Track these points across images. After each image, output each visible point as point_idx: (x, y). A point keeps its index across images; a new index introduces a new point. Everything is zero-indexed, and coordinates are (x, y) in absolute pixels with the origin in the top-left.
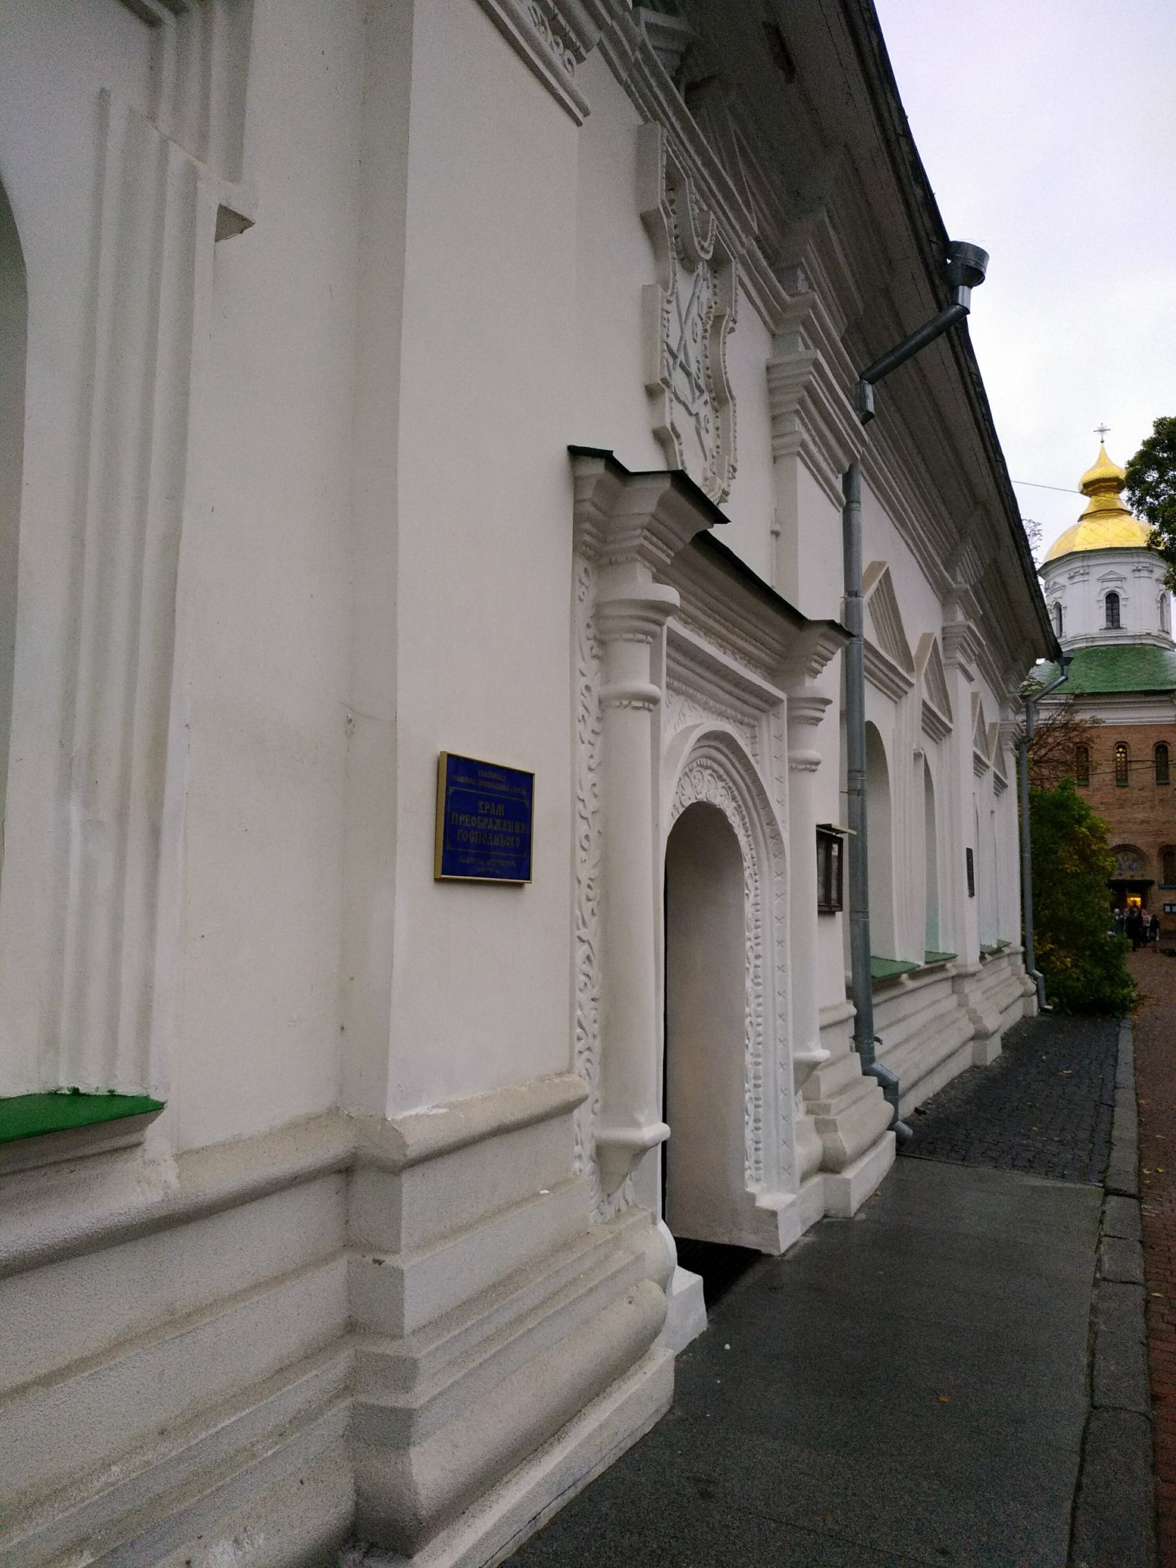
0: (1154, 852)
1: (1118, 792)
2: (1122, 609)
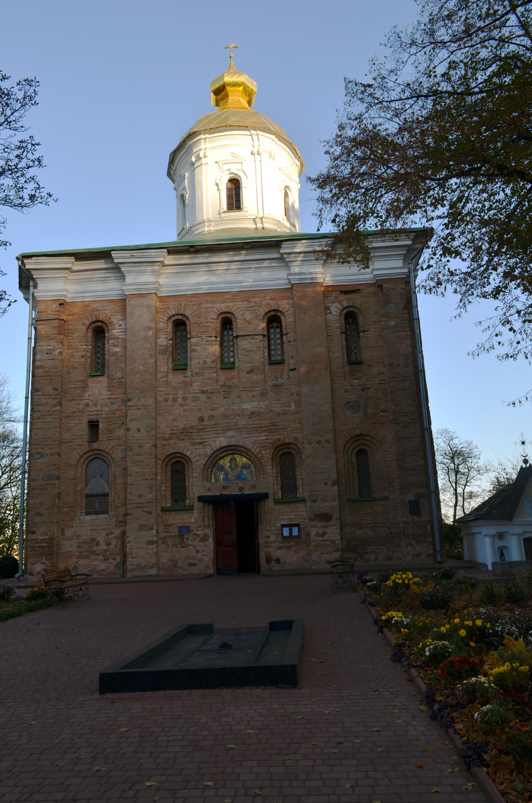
0: (267, 454)
1: (223, 376)
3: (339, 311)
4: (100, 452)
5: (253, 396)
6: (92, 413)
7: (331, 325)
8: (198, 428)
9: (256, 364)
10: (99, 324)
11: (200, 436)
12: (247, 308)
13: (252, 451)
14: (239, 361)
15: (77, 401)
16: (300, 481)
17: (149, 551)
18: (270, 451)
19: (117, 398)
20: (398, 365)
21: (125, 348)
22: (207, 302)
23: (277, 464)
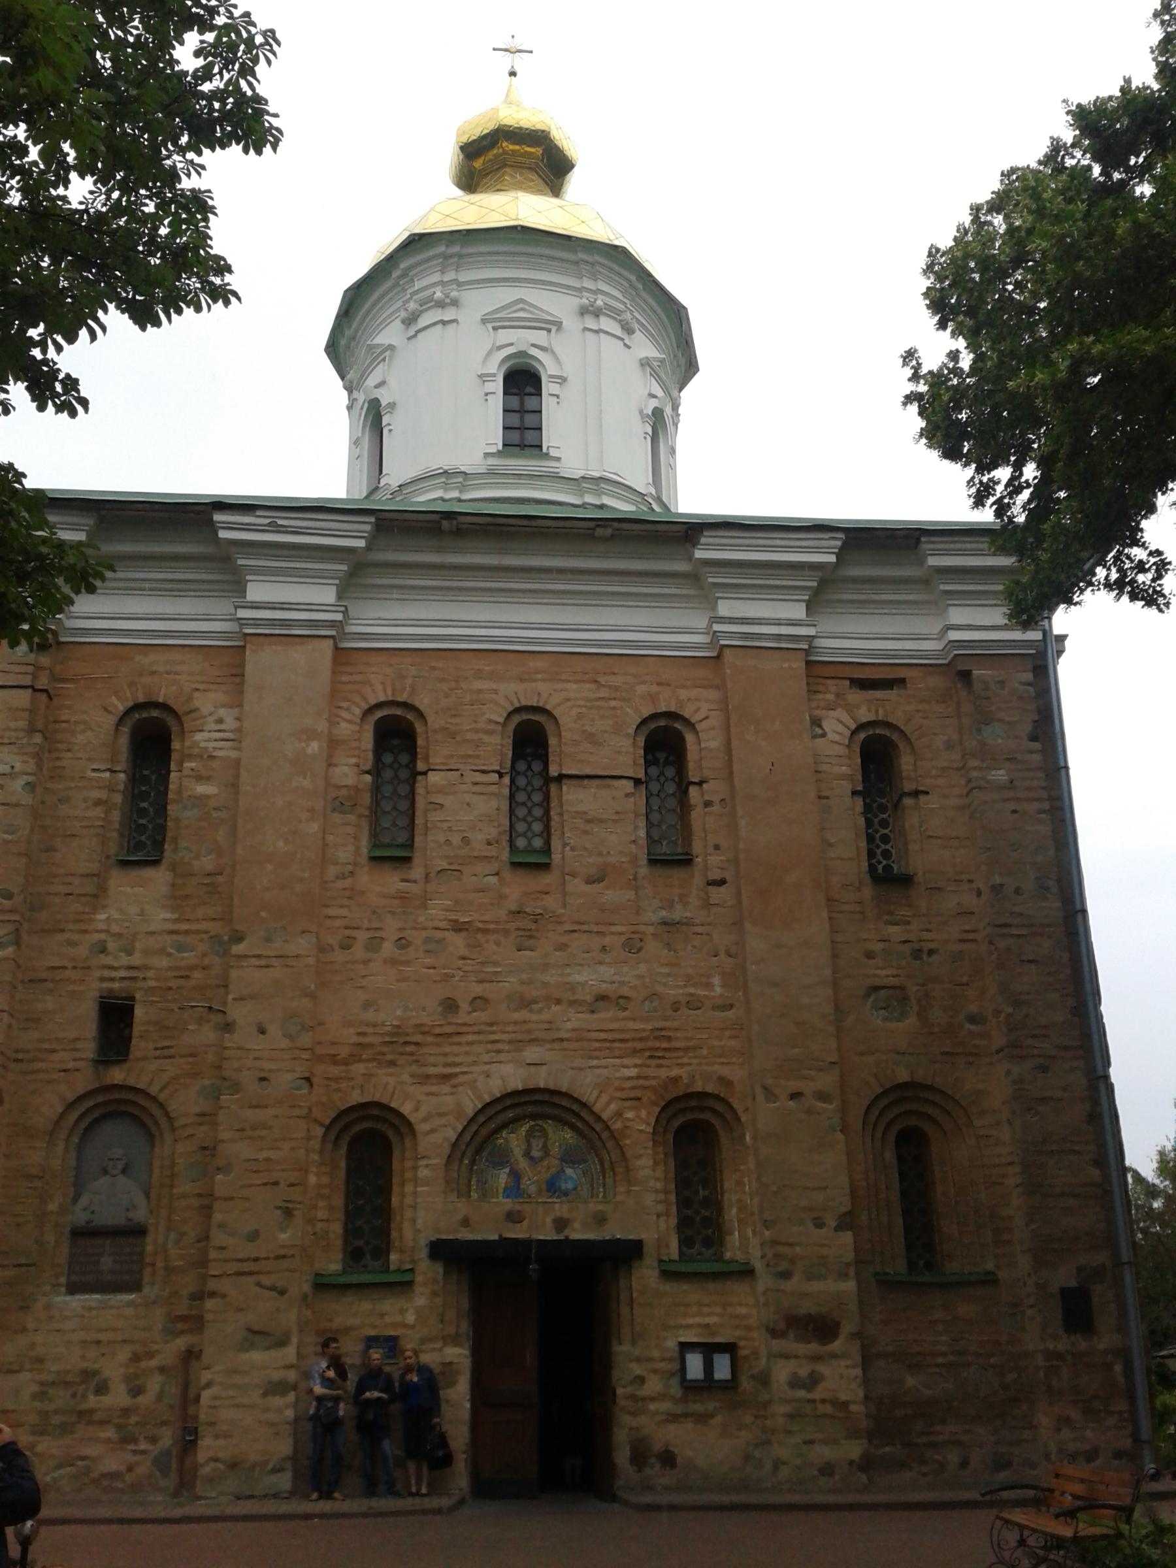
1: (516, 888)
2: (548, 403)
3: (848, 733)
4: (130, 1096)
5: (603, 949)
6: (114, 974)
7: (824, 767)
8: (438, 1030)
9: (613, 859)
10: (155, 713)
11: (445, 1055)
12: (591, 700)
13: (597, 1108)
14: (565, 845)
15: (68, 935)
16: (734, 1211)
17: (270, 1416)
18: (648, 1114)
19: (198, 932)
20: (1018, 891)
21: (234, 786)
22: (479, 675)
23: (666, 1154)
